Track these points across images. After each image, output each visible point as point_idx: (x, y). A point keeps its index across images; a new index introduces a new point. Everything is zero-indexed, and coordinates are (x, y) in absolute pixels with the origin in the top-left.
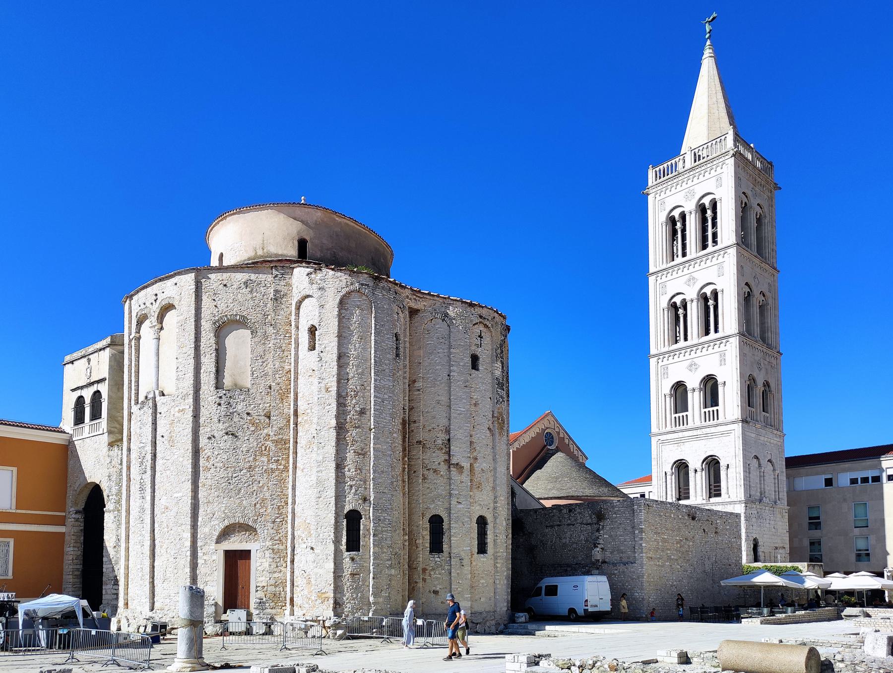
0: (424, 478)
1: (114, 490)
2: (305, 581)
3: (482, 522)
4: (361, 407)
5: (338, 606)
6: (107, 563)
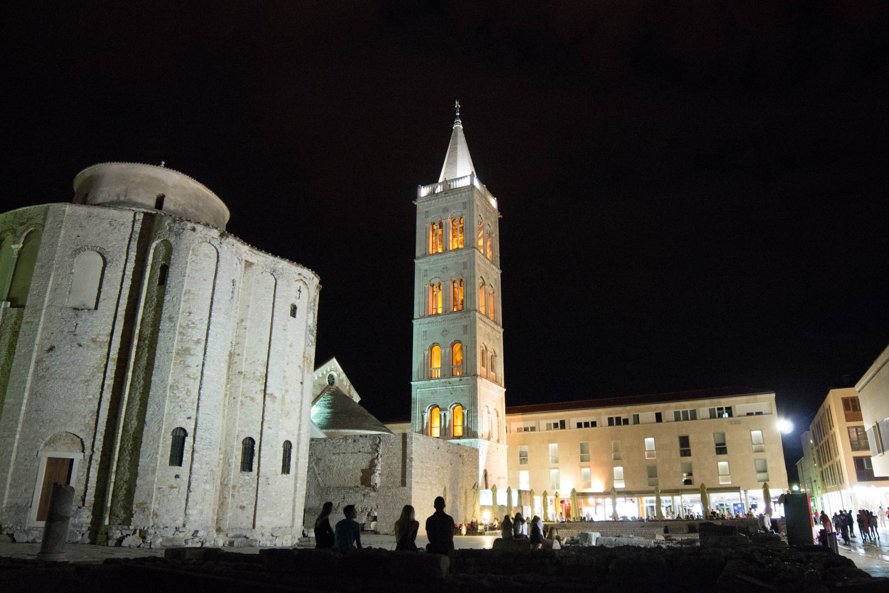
0: (242, 405)
3: (288, 446)
4: (198, 338)
5: (154, 517)
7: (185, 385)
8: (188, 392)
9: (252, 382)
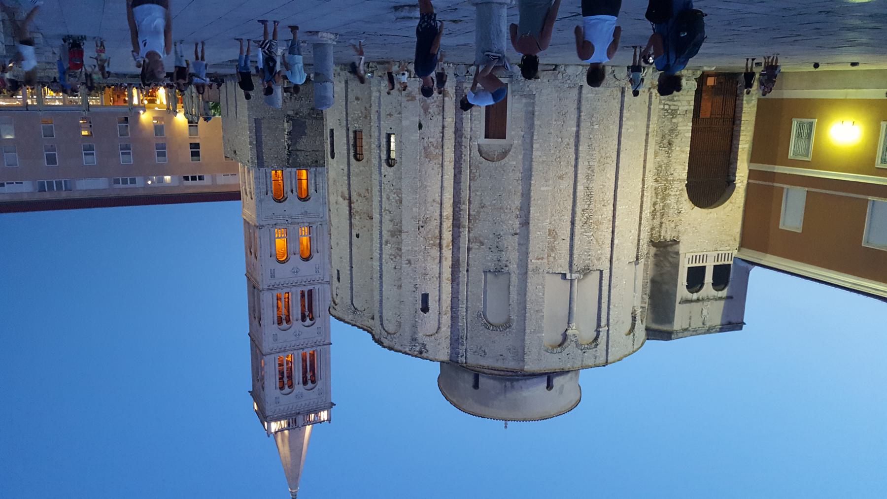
1: (671, 201)
2: (429, 110)
4: (387, 246)
6: (686, 131)
7: (391, 204)
8: (388, 199)
9: (361, 210)
